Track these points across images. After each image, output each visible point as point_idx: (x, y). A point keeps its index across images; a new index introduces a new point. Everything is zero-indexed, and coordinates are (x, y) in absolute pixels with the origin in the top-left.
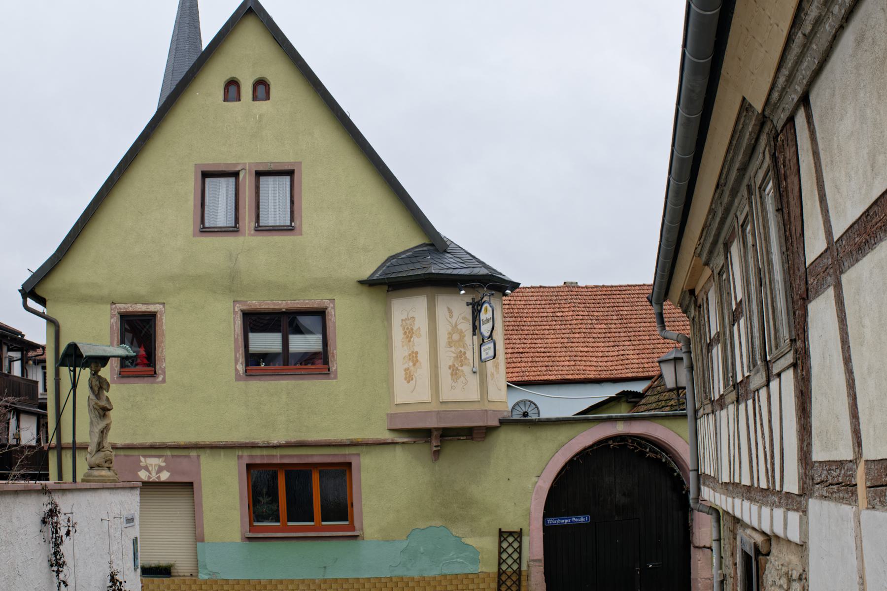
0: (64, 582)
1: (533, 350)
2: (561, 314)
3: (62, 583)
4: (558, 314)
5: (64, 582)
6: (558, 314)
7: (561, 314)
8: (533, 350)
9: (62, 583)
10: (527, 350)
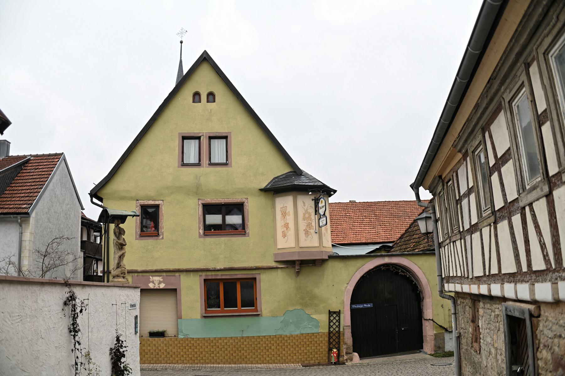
1: (337, 230)
2: (349, 214)
4: (348, 214)
6: (348, 214)
7: (349, 214)
8: (337, 230)
10: (334, 230)
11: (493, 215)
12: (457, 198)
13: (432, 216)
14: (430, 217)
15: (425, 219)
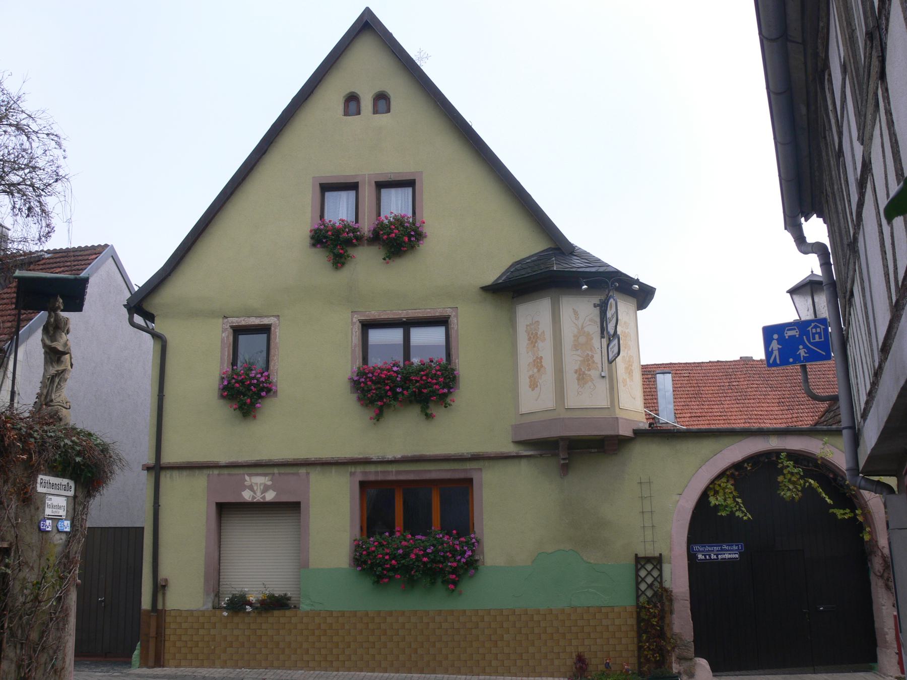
1: (710, 414)
2: (737, 383)
4: (734, 384)
6: (734, 384)
7: (737, 383)
8: (710, 414)
10: (704, 414)
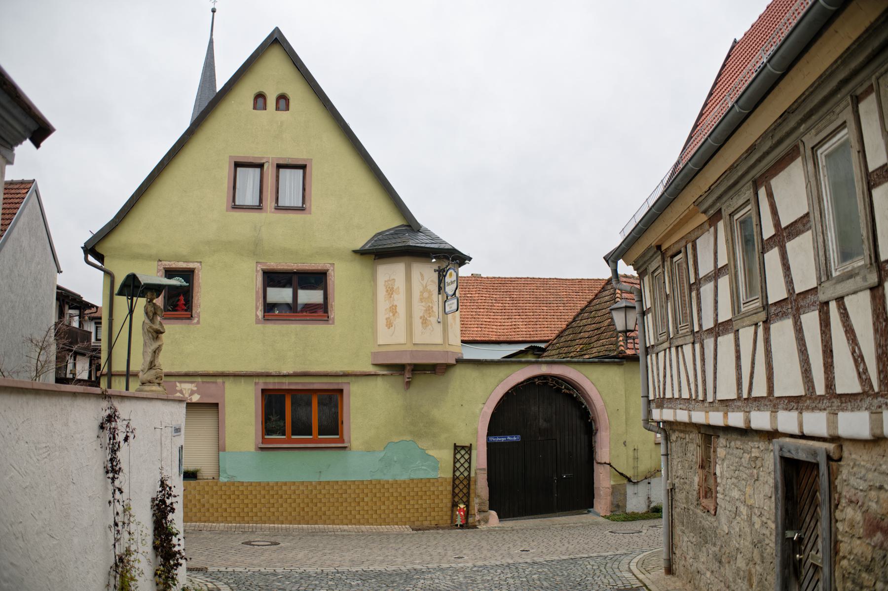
0: (120, 490)
2: (471, 295)
3: (117, 490)
4: (469, 295)
5: (120, 490)
6: (469, 295)
7: (471, 295)
9: (117, 490)
11: (764, 310)
12: (692, 281)
13: (637, 305)
14: (634, 308)
15: (624, 309)
